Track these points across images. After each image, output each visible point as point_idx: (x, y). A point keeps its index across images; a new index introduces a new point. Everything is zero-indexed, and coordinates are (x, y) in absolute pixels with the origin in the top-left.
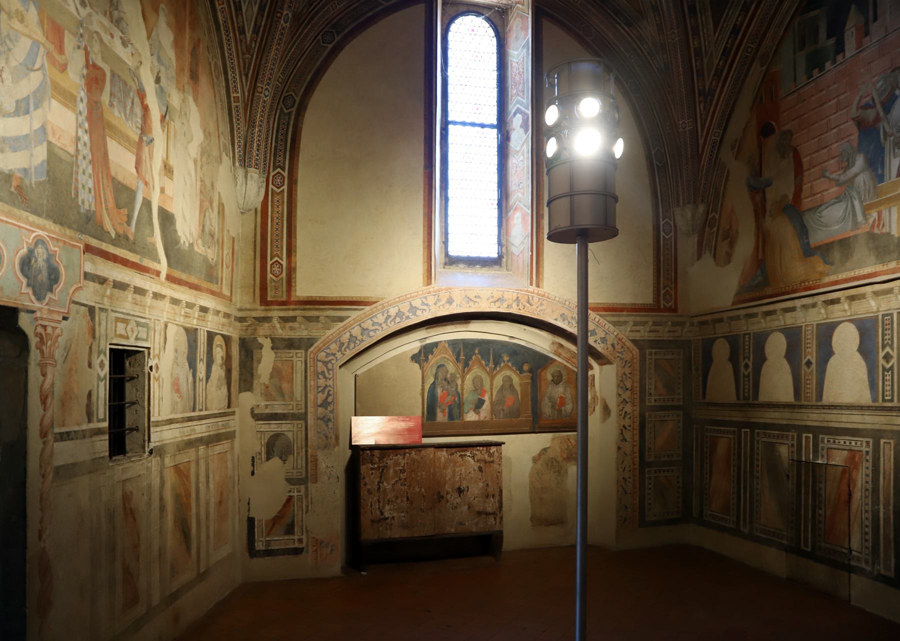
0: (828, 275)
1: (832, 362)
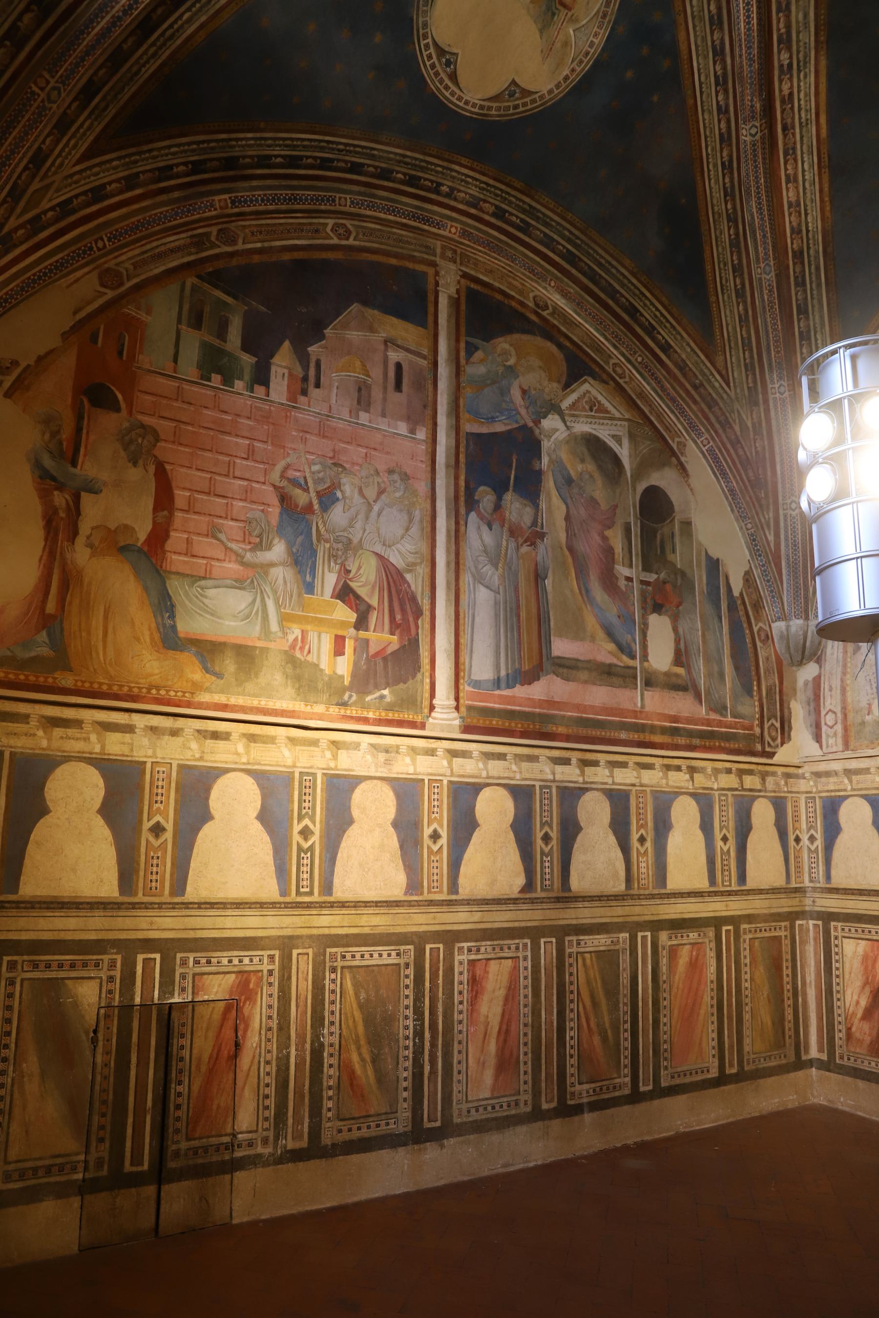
0: (208, 690)
1: (207, 832)
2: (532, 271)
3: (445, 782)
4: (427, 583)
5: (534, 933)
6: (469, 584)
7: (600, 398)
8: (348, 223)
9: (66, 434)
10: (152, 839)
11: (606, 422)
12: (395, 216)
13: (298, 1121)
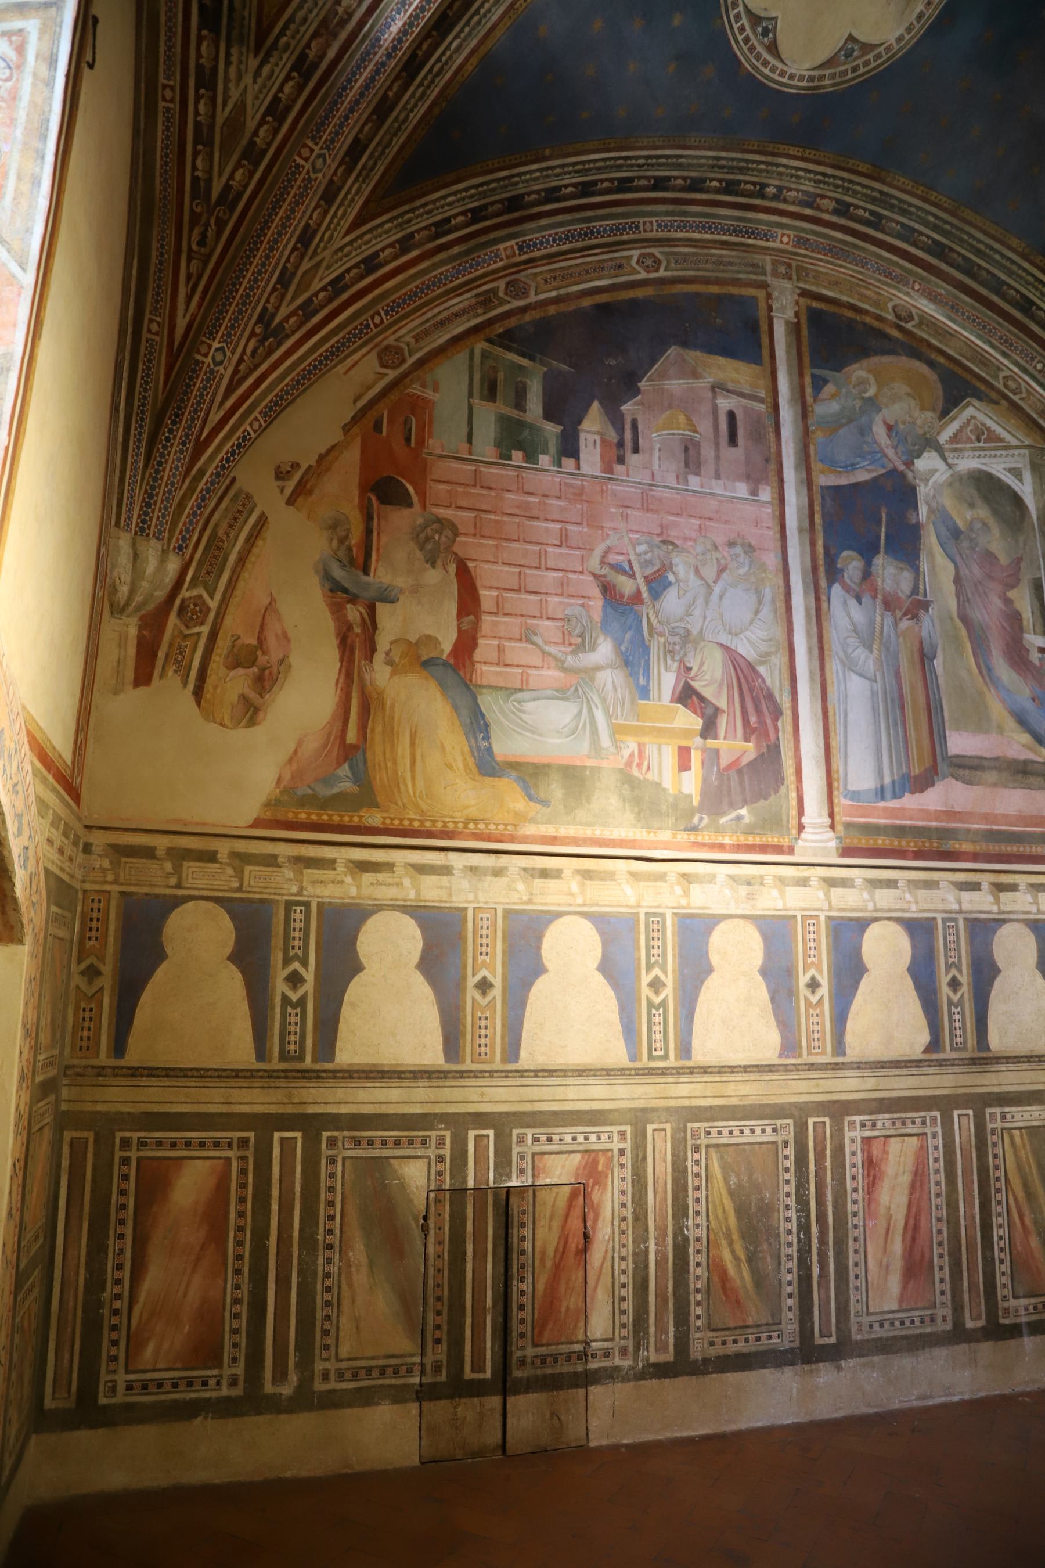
0: (533, 821)
1: (540, 987)
2: (889, 275)
3: (822, 919)
4: (786, 675)
5: (945, 1104)
6: (837, 672)
7: (989, 423)
8: (656, 251)
9: (356, 538)
10: (478, 997)
11: (999, 453)
12: (712, 233)
13: (662, 1329)
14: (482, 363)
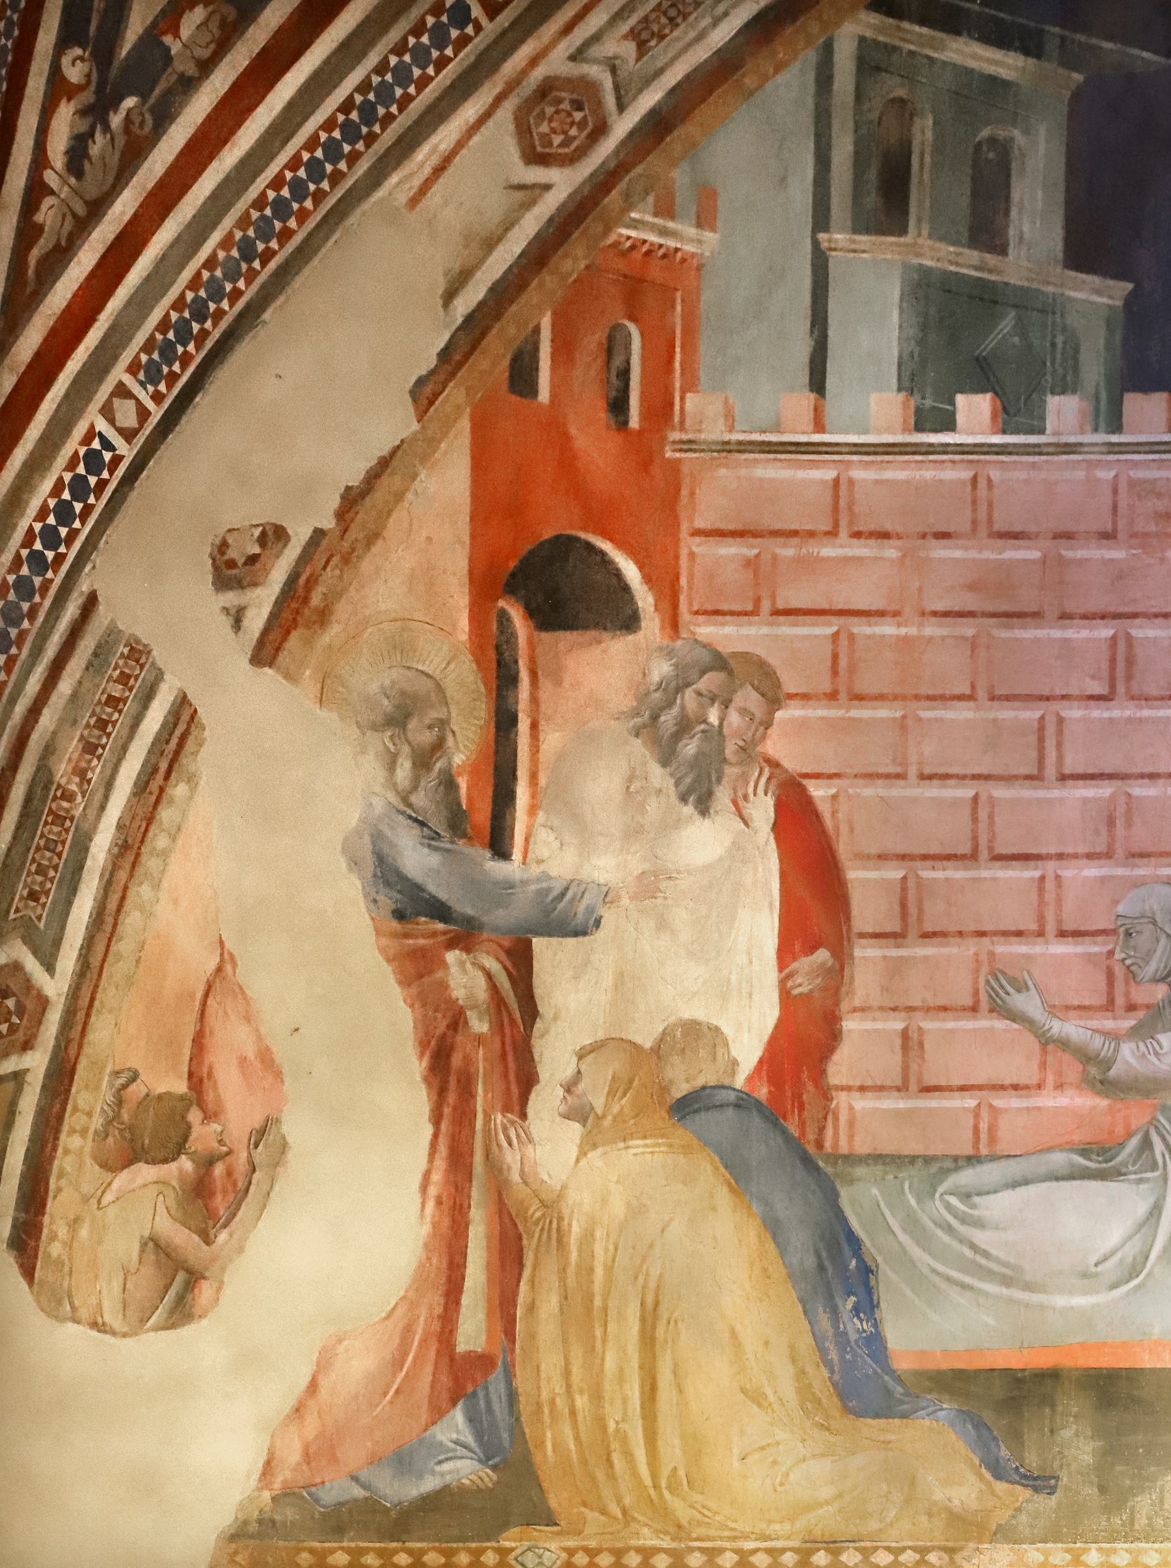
14: (859, 96)
